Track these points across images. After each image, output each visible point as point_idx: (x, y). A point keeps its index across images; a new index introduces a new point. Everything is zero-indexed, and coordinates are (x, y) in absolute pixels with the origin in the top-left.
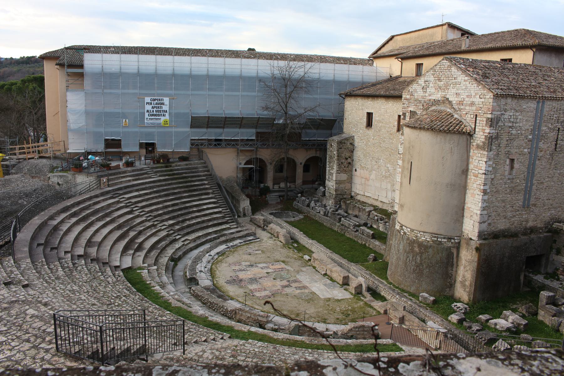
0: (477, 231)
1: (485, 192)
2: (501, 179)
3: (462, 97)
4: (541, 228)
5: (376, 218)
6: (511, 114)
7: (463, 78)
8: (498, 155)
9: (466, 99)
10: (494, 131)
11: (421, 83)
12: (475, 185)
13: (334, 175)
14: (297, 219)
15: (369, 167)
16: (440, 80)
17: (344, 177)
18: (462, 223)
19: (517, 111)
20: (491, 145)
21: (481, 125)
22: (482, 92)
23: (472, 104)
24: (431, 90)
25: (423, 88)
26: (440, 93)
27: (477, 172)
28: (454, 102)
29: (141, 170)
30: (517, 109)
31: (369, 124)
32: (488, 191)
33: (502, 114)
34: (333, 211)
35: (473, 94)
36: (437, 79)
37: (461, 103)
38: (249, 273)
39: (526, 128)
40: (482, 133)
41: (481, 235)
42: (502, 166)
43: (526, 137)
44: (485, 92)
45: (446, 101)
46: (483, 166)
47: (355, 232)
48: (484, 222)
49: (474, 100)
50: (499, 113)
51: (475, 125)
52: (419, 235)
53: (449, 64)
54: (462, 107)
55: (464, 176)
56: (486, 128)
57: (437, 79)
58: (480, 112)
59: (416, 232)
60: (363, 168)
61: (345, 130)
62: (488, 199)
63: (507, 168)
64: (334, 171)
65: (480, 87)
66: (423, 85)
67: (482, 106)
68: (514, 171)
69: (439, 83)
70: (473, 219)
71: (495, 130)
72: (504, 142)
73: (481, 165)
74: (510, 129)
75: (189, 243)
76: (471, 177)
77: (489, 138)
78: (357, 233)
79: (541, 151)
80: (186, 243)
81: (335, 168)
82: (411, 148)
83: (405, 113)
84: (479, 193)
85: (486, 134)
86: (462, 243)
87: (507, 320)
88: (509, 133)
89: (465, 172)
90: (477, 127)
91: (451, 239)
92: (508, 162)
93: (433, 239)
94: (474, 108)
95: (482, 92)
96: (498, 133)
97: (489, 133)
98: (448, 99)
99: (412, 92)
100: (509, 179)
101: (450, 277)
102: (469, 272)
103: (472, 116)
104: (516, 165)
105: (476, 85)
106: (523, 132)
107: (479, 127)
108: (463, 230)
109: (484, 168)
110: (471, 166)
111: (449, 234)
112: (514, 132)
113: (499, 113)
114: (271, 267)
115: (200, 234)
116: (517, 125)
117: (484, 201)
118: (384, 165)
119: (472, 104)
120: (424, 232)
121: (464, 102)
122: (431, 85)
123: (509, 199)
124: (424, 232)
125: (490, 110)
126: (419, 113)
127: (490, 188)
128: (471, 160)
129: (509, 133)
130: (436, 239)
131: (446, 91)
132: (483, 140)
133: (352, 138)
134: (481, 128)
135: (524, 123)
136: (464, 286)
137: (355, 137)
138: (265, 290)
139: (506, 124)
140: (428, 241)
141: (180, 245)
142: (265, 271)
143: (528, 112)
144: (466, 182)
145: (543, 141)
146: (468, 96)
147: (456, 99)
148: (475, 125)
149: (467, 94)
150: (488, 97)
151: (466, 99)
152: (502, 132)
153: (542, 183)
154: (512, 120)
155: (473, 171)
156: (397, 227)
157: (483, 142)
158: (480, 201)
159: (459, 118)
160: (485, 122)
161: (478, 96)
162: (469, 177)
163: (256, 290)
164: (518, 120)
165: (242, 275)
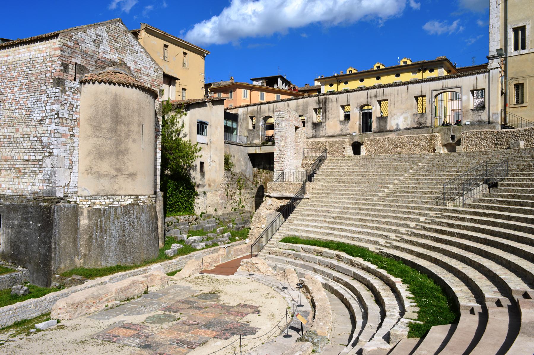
3: (139, 66)
11: (91, 34)
23: (148, 75)
24: (104, 47)
28: (132, 69)
35: (149, 67)
37: (139, 71)
45: (123, 64)
54: (140, 75)
67: (155, 78)
82: (142, 109)
83: (67, 65)
98: (125, 64)
126: (91, 69)
146: (144, 67)
147: (134, 67)
151: (143, 69)
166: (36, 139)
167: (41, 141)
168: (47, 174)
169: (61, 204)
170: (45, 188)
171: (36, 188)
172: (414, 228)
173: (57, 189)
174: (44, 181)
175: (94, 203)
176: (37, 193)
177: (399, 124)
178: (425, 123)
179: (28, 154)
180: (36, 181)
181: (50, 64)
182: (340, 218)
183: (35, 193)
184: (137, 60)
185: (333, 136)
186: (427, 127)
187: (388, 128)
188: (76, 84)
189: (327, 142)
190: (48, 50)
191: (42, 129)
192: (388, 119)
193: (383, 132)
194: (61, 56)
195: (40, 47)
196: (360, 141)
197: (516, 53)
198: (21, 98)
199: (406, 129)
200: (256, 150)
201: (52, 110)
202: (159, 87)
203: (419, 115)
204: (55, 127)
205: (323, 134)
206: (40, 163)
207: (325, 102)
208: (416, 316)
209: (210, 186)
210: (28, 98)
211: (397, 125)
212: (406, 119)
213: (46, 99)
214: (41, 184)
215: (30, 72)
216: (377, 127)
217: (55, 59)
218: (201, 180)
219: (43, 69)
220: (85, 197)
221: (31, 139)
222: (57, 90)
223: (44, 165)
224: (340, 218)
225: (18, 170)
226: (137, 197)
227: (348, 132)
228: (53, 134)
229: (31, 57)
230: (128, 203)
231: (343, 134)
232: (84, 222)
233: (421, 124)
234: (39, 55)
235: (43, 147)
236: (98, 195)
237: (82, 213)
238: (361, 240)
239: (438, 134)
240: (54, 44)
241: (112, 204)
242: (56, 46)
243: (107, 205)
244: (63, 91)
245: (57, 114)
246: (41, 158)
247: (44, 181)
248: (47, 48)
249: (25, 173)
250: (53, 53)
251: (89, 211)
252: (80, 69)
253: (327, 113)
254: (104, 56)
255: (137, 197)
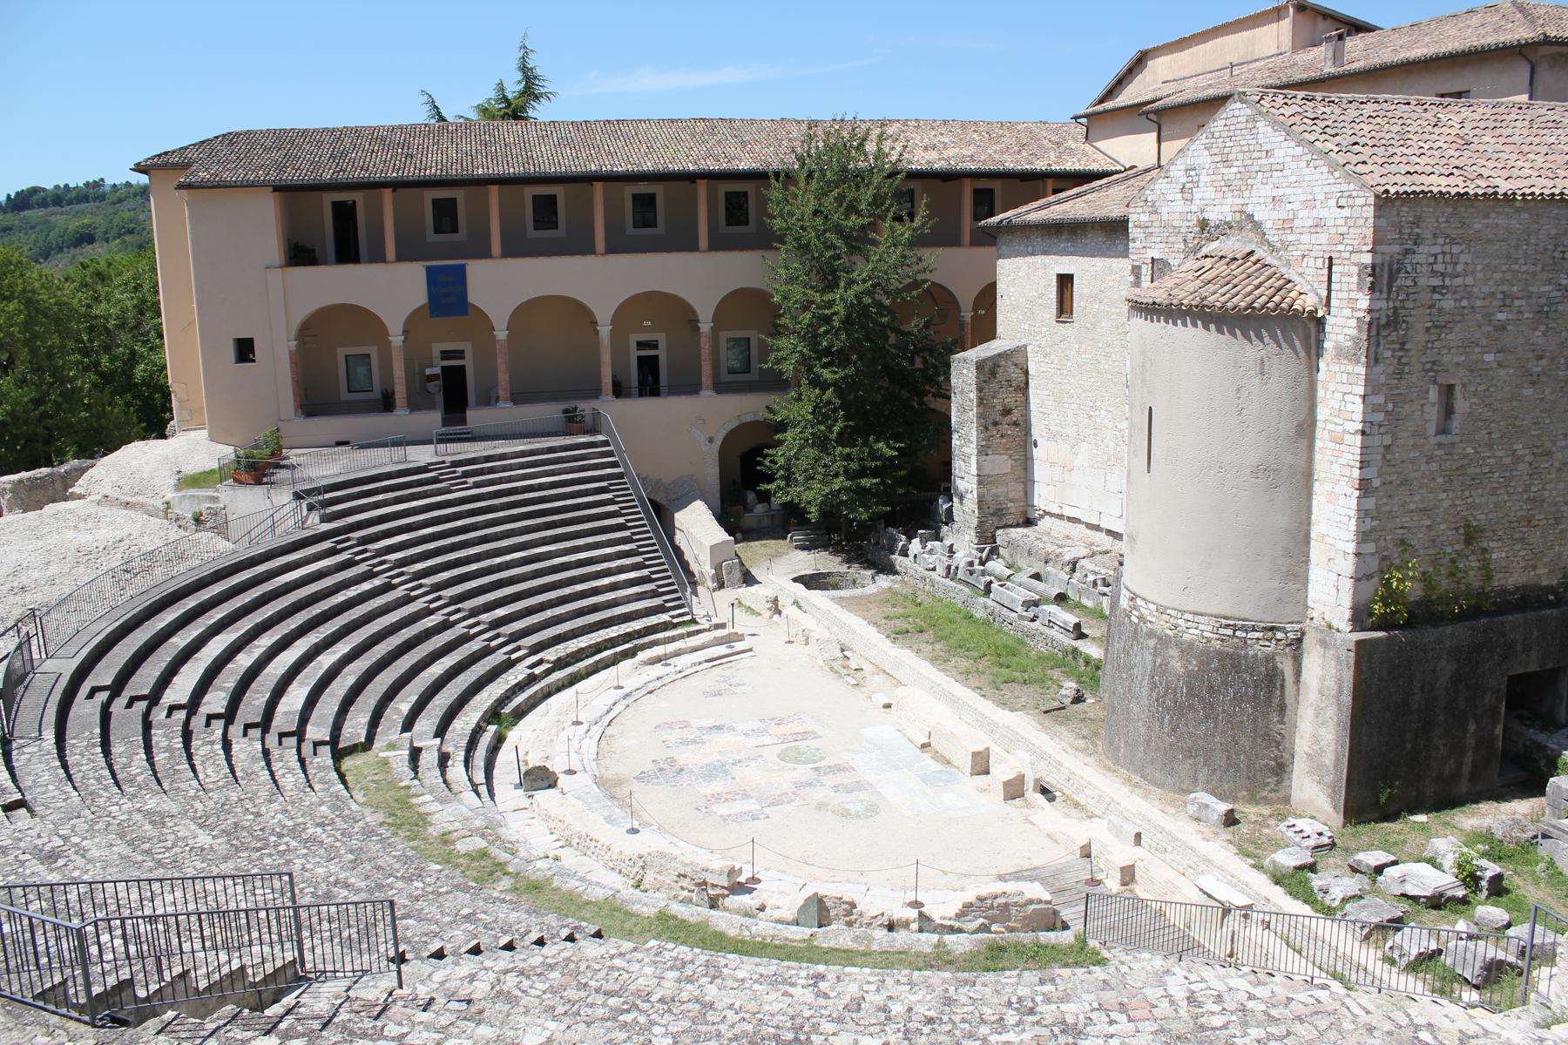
0: (1347, 602)
1: (1364, 486)
2: (1415, 446)
4: (1550, 589)
5: (1091, 578)
6: (1437, 249)
7: (1290, 152)
8: (1399, 374)
9: (1302, 214)
10: (1383, 304)
12: (1336, 468)
13: (974, 460)
14: (871, 589)
15: (1071, 431)
16: (1226, 162)
17: (1002, 464)
18: (1306, 582)
19: (1453, 242)
20: (1378, 344)
21: (1345, 287)
22: (1345, 187)
24: (1204, 194)
25: (1182, 190)
26: (1229, 201)
27: (1340, 429)
28: (1269, 224)
29: (424, 469)
30: (1453, 233)
31: (1064, 306)
32: (1376, 483)
33: (1407, 252)
34: (971, 564)
35: (1320, 197)
36: (1218, 158)
37: (1287, 225)
38: (707, 749)
39: (1485, 289)
40: (1348, 312)
41: (1360, 618)
42: (1416, 406)
43: (1489, 318)
44: (1352, 186)
46: (1356, 409)
47: (1033, 620)
48: (1369, 577)
49: (1323, 213)
50: (1397, 248)
51: (1329, 290)
52: (1180, 622)
53: (1249, 112)
54: (1291, 238)
55: (1304, 443)
56: (1360, 295)
57: (1218, 158)
58: (1341, 247)
59: (1173, 613)
60: (1053, 436)
61: (1000, 330)
62: (1378, 507)
63: (1433, 413)
64: (972, 449)
65: (1337, 174)
66: (1184, 180)
67: (1344, 230)
68: (1456, 423)
69: (1224, 171)
70: (1337, 569)
71: (1388, 299)
72: (1417, 338)
73: (1350, 407)
74: (1437, 296)
75: (548, 672)
76: (1322, 441)
77: (1370, 324)
78: (1033, 625)
79: (1540, 358)
80: (537, 671)
81: (974, 438)
82: (1148, 366)
83: (1139, 268)
84: (1349, 491)
85: (1361, 314)
86: (1306, 640)
87: (1438, 867)
88: (1432, 306)
89: (1306, 429)
90: (1333, 294)
91: (1272, 629)
92: (1434, 394)
93: (1222, 631)
94: (1323, 238)
95: (1345, 187)
96: (1395, 308)
97: (1370, 311)
99: (1154, 203)
100: (1439, 445)
101: (1278, 744)
102: (1331, 725)
103: (1319, 263)
104: (1461, 405)
105: (1325, 169)
106: (1479, 303)
107: (1341, 295)
108: (1310, 603)
109: (1359, 416)
110: (1322, 412)
111: (1269, 619)
112: (1448, 304)
113: (1397, 248)
114: (773, 729)
115: (583, 645)
116: (1458, 281)
117: (1363, 513)
118: (1110, 425)
119: (1318, 226)
120: (1195, 614)
121: (1297, 223)
122: (1204, 178)
123: (1446, 504)
124: (1195, 614)
125: (1370, 240)
127: (1380, 476)
128: (1320, 393)
129: (1432, 306)
130: (1230, 632)
131: (1246, 193)
132: (1354, 332)
133: (1021, 351)
134: (1345, 295)
135: (1479, 275)
136: (1317, 770)
137: (1029, 349)
138: (746, 795)
139: (1422, 282)
140: (1209, 640)
141: (521, 677)
142: (754, 742)
143: (1489, 241)
144: (1310, 460)
145: (1543, 328)
146: (1309, 204)
147: (1274, 215)
148: (1329, 290)
149: (1303, 198)
150: (1360, 201)
152: (1409, 305)
153: (1549, 454)
154: (1439, 267)
155: (1330, 426)
156: (1124, 603)
157: (1353, 338)
158: (1353, 513)
159: (1283, 270)
160: (1355, 279)
161: (1332, 202)
162: (1318, 444)
163: (718, 798)
164: (1460, 268)
165: (684, 756)
184: (1281, 192)
202: (1356, 258)
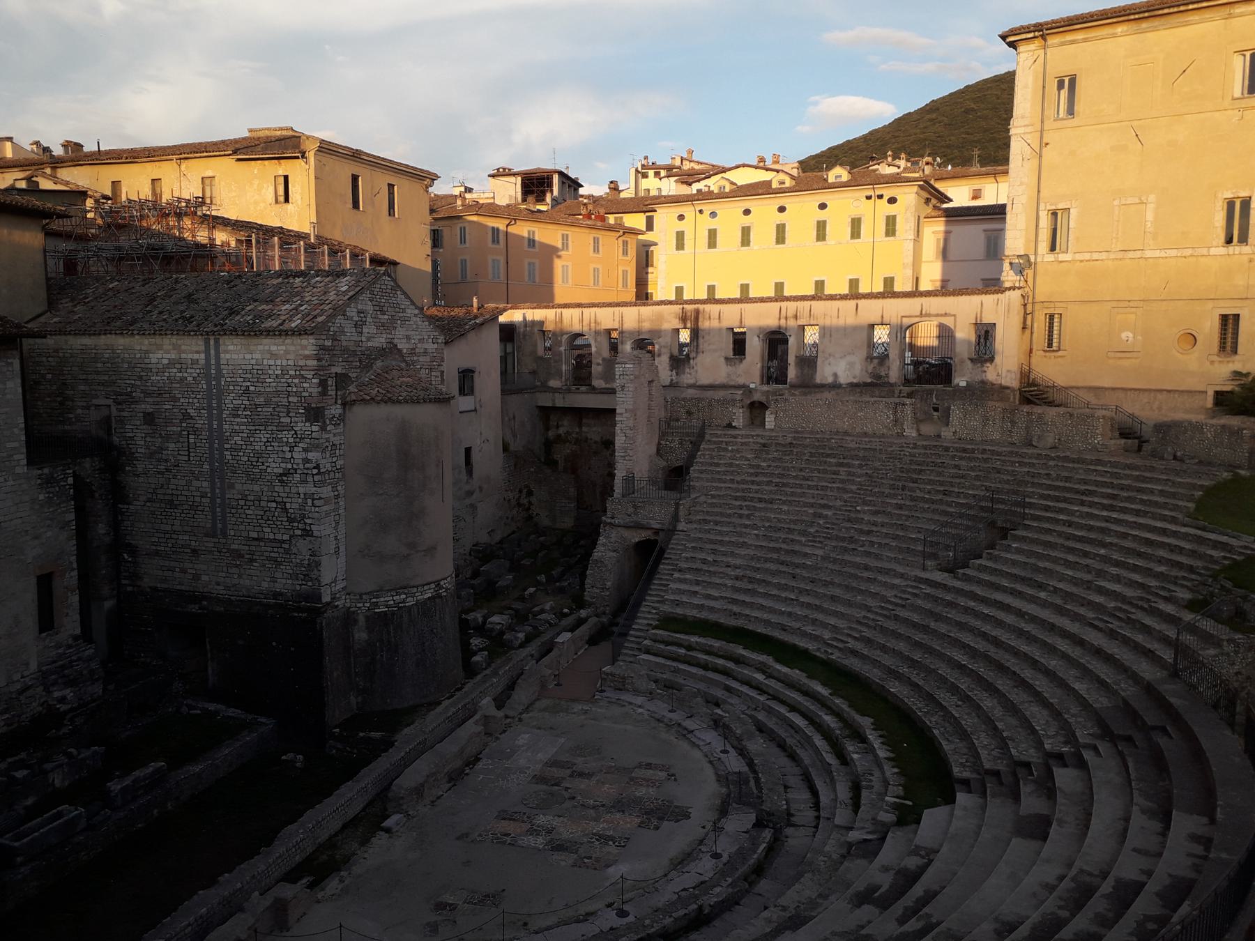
23: (425, 353)
24: (369, 329)
37: (412, 351)
45: (392, 349)
49: (426, 346)
119: (425, 353)
166: (274, 505)
167: (285, 510)
168: (302, 565)
169: (329, 614)
170: (298, 588)
171: (278, 587)
172: (876, 613)
173: (323, 590)
174: (294, 576)
175: (376, 605)
176: (281, 594)
177: (840, 373)
178: (887, 376)
179: (258, 529)
180: (278, 575)
181: (296, 381)
182: (751, 580)
183: (276, 595)
185: (711, 387)
186: (891, 385)
187: (818, 380)
188: (336, 410)
189: (700, 400)
190: (291, 356)
191: (287, 489)
192: (819, 363)
193: (807, 386)
194: (319, 369)
195: (274, 348)
196: (763, 399)
197: (1051, 257)
198: (237, 432)
199: (852, 385)
200: (553, 401)
201: (306, 461)
203: (876, 361)
204: (313, 490)
205: (692, 381)
206: (286, 546)
207: (697, 318)
208: (900, 791)
209: (481, 489)
210: (252, 433)
211: (835, 375)
212: (851, 365)
213: (291, 440)
214: (289, 582)
215: (252, 388)
216: (797, 377)
217: (309, 375)
218: (467, 482)
219: (282, 387)
220: (361, 595)
221: (263, 504)
222: (315, 428)
223: (294, 550)
224: (751, 580)
225: (237, 554)
226: (438, 583)
227: (741, 381)
228: (309, 501)
229: (253, 362)
230: (426, 596)
231: (732, 383)
232: (361, 635)
233: (880, 377)
234: (271, 362)
235: (291, 520)
236: (381, 590)
237: (356, 621)
238: (794, 631)
239: (908, 401)
240: (305, 347)
241: (404, 602)
242: (307, 352)
243: (396, 604)
244: (323, 428)
245: (317, 467)
246: (286, 537)
247: (294, 576)
248: (287, 352)
249: (252, 560)
250: (302, 363)
251: (367, 618)
252: (342, 380)
253: (701, 340)
254: (370, 344)
255: (438, 583)
